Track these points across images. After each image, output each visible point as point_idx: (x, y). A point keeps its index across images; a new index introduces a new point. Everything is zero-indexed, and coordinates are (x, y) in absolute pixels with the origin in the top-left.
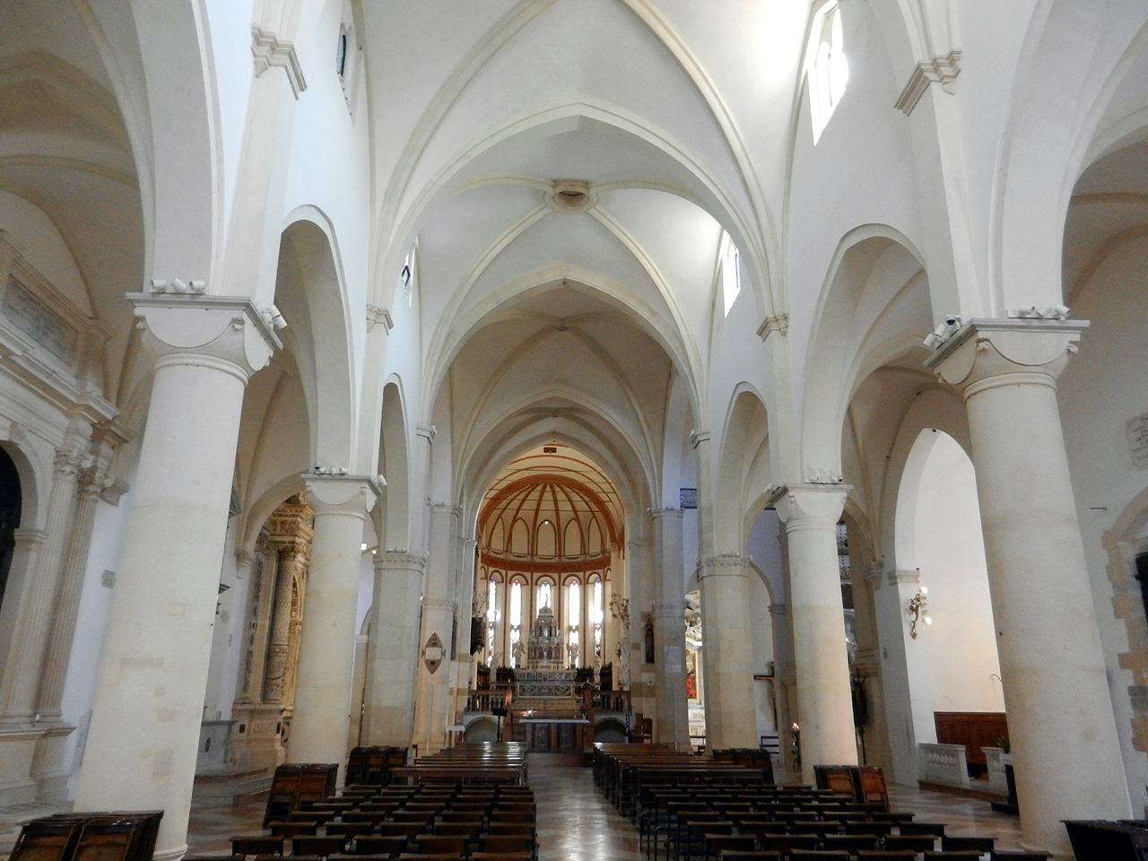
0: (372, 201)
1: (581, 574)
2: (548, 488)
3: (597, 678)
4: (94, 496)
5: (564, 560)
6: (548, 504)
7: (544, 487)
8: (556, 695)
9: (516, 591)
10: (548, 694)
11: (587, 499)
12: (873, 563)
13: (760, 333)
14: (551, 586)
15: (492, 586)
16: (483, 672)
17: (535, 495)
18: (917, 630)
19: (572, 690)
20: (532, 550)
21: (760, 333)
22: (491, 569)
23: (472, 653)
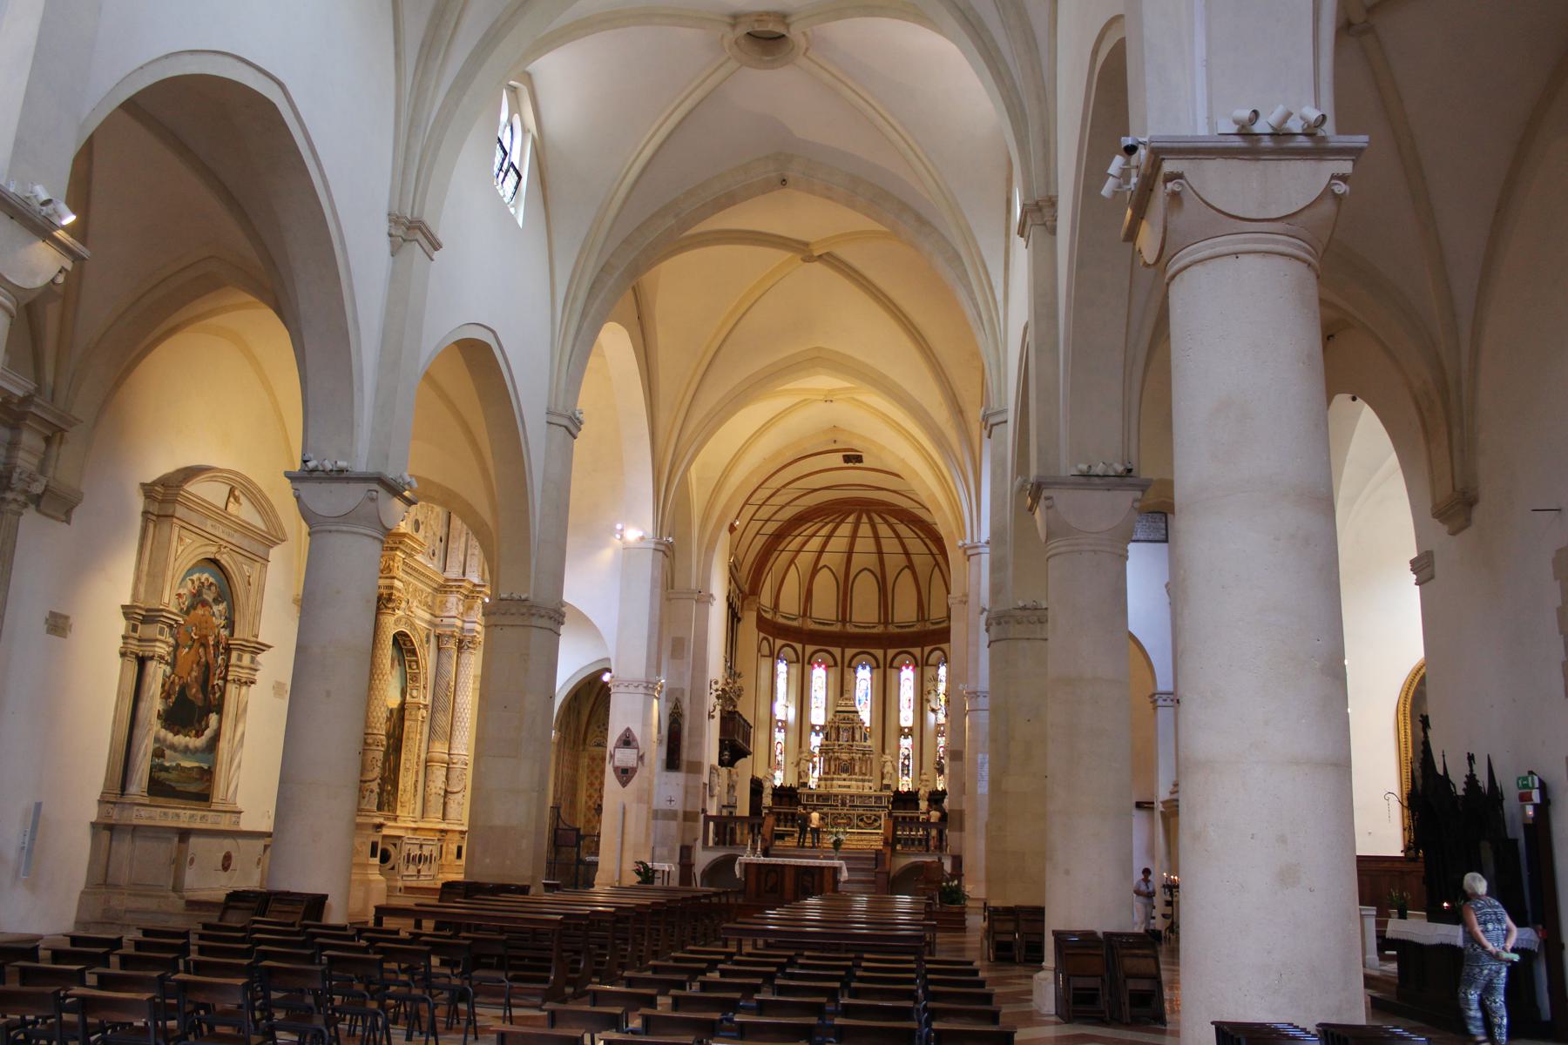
0: (398, 56)
1: (917, 651)
4: (14, 506)
5: (892, 629)
6: (865, 544)
8: (858, 827)
9: (819, 676)
14: (827, 668)
15: (782, 667)
16: (757, 787)
17: (845, 529)
20: (844, 613)
22: (779, 643)
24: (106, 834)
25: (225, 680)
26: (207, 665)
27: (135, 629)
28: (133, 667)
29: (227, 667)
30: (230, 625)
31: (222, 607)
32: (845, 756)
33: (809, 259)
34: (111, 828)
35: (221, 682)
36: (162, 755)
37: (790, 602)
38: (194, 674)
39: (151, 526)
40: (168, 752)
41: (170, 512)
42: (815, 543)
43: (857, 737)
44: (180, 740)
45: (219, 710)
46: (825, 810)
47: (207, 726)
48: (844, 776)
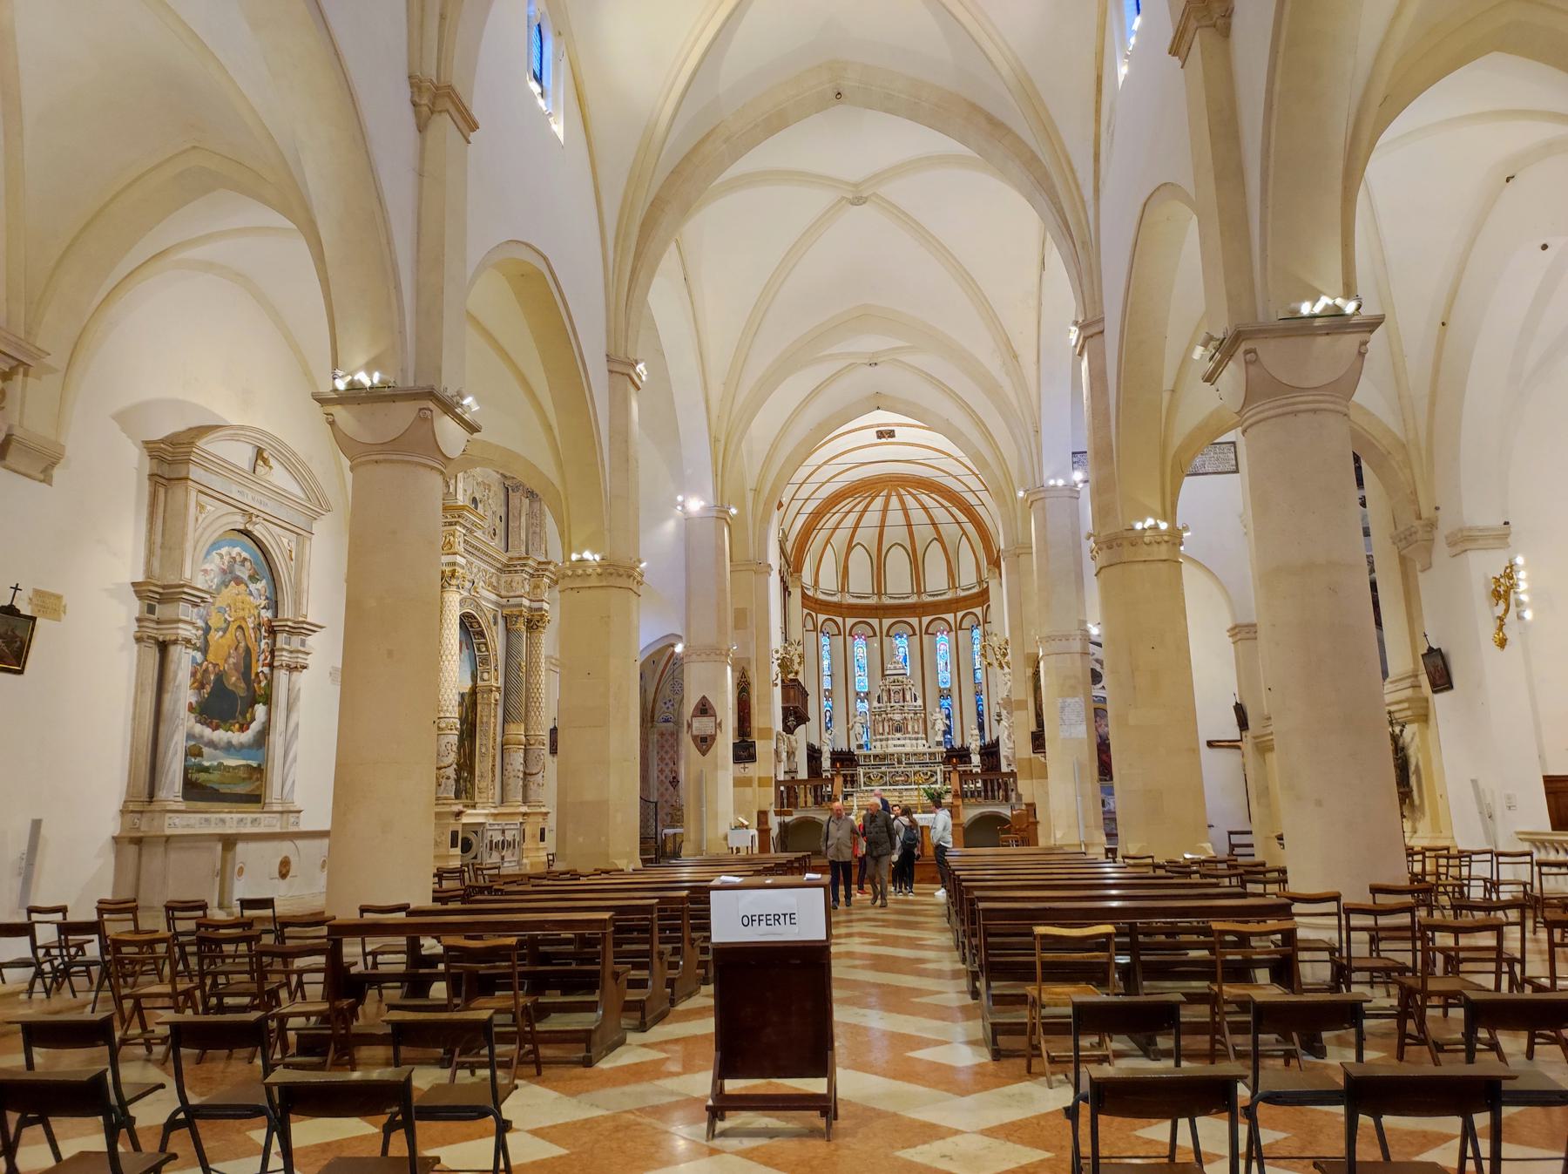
3: (976, 759)
6: (895, 517)
7: (888, 498)
10: (905, 782)
11: (947, 504)
12: (1417, 523)
13: (1174, 51)
16: (814, 754)
18: (1511, 632)
19: (939, 777)
21: (1174, 51)
22: (821, 618)
23: (789, 730)
24: (132, 850)
25: (271, 666)
26: (248, 651)
27: (151, 610)
28: (153, 655)
29: (272, 652)
30: (274, 604)
31: (262, 585)
32: (897, 717)
34: (138, 841)
35: (266, 670)
36: (200, 754)
37: (829, 581)
38: (232, 660)
39: (162, 491)
40: (206, 750)
41: (183, 474)
42: (851, 520)
43: (908, 697)
44: (221, 735)
45: (268, 700)
47: (253, 719)
48: (898, 735)
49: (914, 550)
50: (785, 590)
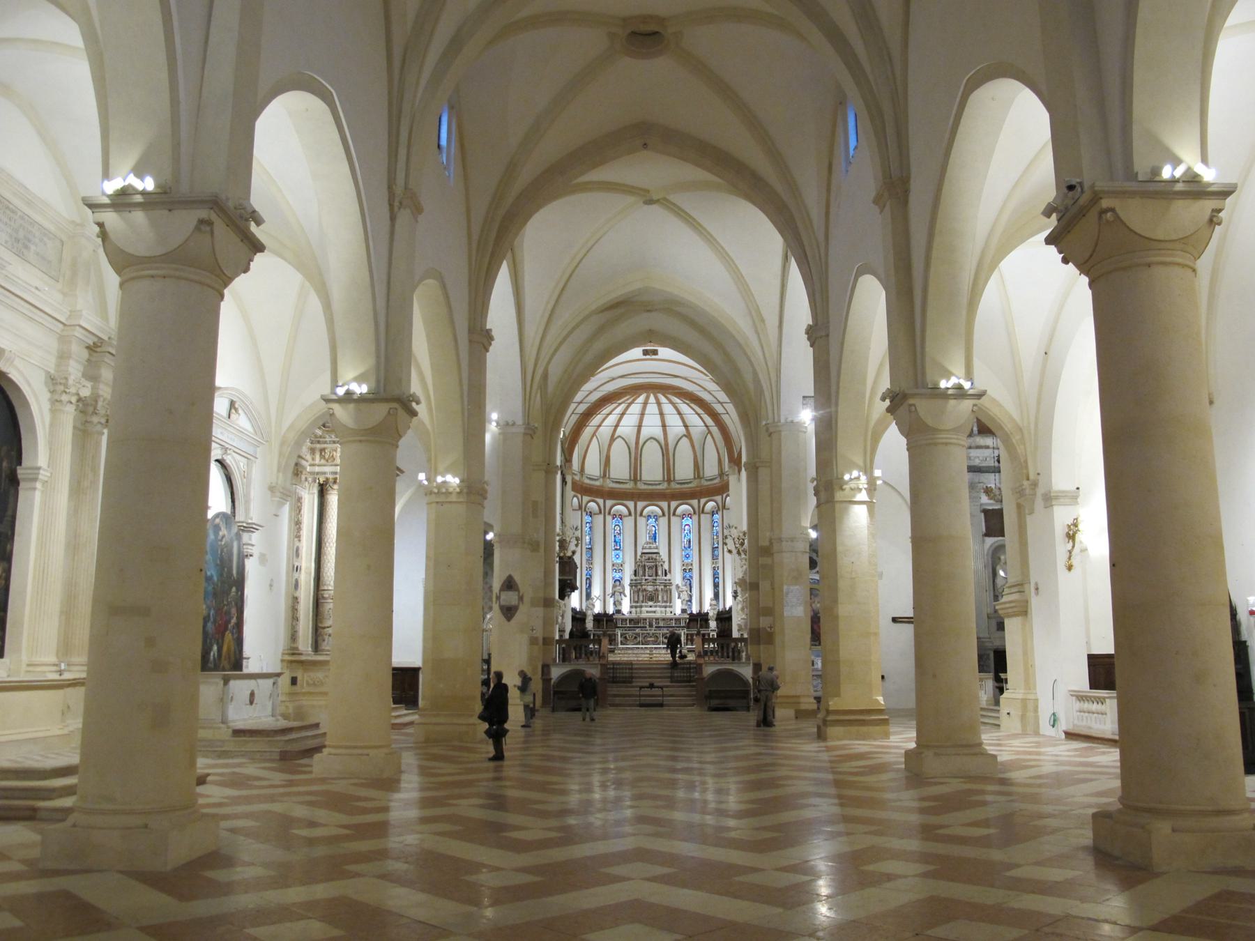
2: (652, 399)
7: (647, 398)
10: (655, 642)
11: (700, 411)
12: (1026, 483)
17: (636, 408)
18: (1074, 561)
22: (586, 499)
23: (563, 595)
32: (650, 588)
33: (650, 202)
37: (593, 467)
42: (611, 420)
46: (638, 631)
49: (667, 444)
50: (564, 481)
